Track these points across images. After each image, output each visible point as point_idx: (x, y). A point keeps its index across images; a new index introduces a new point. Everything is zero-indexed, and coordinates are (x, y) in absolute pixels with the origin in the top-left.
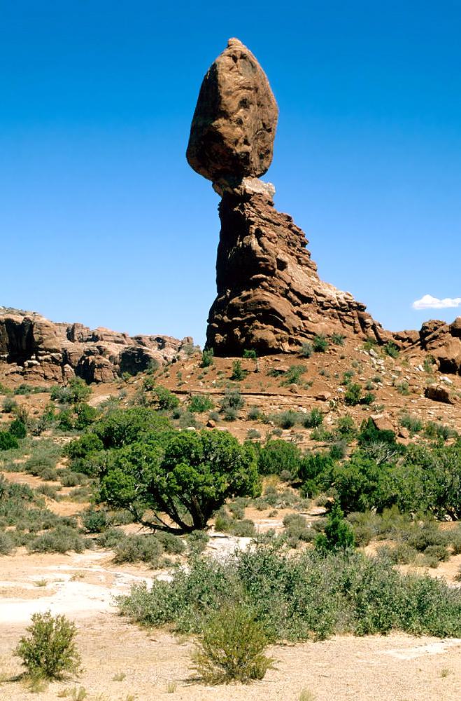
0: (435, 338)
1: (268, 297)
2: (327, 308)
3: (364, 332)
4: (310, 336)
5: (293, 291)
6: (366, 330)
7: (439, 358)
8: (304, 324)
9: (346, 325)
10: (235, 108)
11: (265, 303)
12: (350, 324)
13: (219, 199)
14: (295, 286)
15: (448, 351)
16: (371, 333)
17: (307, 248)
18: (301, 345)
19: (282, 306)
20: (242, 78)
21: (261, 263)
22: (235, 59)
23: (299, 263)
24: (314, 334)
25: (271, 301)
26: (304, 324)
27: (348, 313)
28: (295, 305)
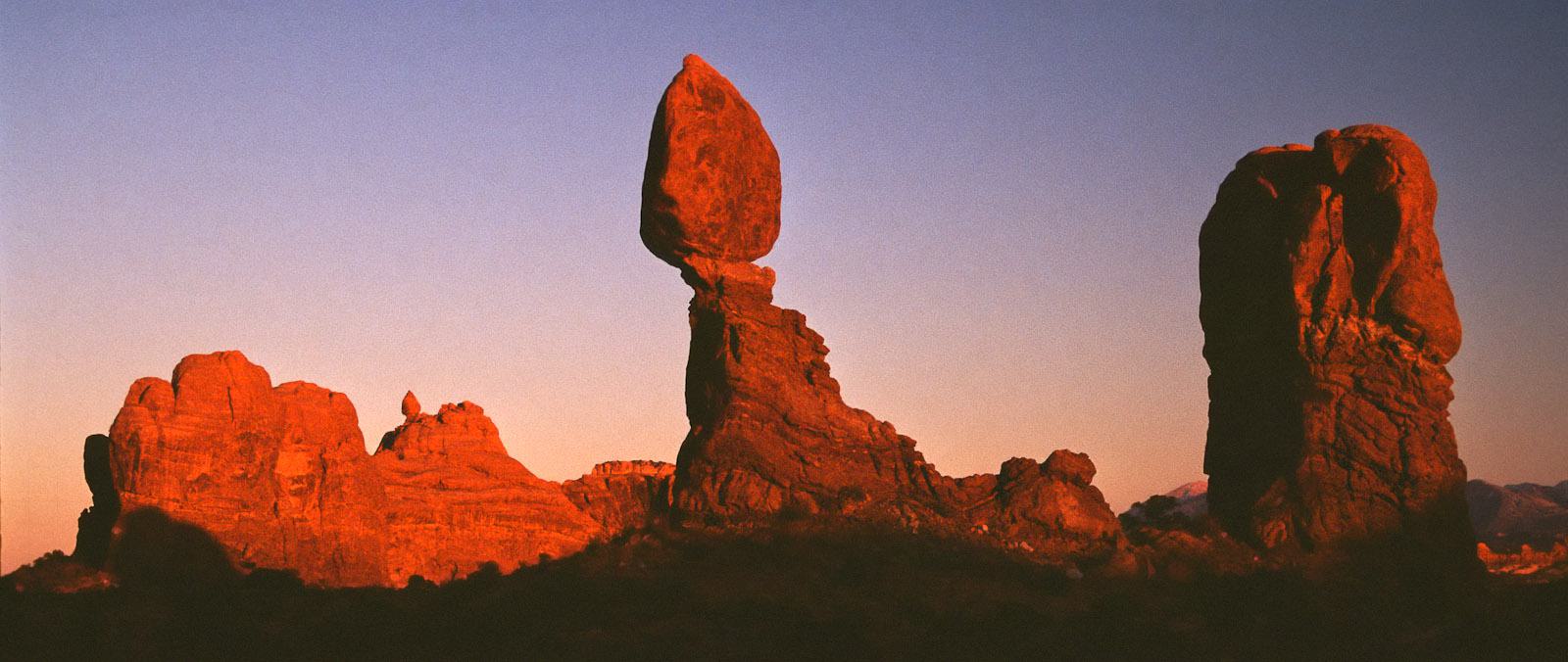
16: (921, 480)
17: (827, 359)
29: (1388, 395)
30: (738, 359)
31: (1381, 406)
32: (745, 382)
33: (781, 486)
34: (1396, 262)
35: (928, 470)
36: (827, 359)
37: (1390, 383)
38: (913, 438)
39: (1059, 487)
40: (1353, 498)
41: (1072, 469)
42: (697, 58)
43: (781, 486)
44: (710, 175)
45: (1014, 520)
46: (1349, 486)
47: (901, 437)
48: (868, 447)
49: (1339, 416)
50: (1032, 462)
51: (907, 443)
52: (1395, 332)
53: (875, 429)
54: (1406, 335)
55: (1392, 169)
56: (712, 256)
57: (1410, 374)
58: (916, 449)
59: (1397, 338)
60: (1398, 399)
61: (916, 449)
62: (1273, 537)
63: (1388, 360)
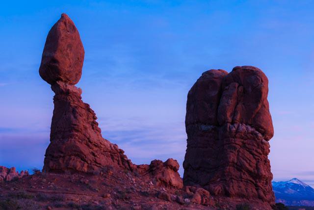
0: (158, 168)
1: (78, 144)
2: (106, 152)
3: (123, 164)
4: (98, 165)
5: (90, 141)
6: (124, 163)
7: (160, 179)
8: (95, 159)
9: (115, 161)
10: (66, 48)
11: (77, 147)
12: (116, 160)
13: (54, 94)
14: (91, 139)
15: (163, 175)
16: (127, 165)
17: (96, 121)
18: (93, 169)
19: (86, 151)
20: (69, 33)
21: (76, 126)
22: (65, 23)
23: (93, 128)
24: (100, 164)
25: (80, 146)
26: (95, 159)
27: (116, 154)
28: (91, 148)
29: (253, 149)
30: (75, 117)
31: (251, 153)
32: (78, 126)
33: (88, 163)
34: (259, 108)
35: (128, 162)
36: (96, 121)
37: (254, 146)
38: (124, 150)
39: (170, 171)
40: (242, 181)
41: (174, 165)
42: (66, 15)
43: (88, 163)
44: (69, 54)
45: (157, 181)
46: (241, 178)
47: (120, 150)
48: (110, 152)
49: (238, 155)
50: (161, 162)
51: (121, 152)
52: (257, 130)
53: (112, 146)
54: (260, 132)
55: (259, 80)
56: (65, 82)
57: (260, 144)
58: (124, 154)
59: (257, 132)
60: (256, 151)
61: (124, 154)
62: (217, 192)
63: (254, 139)
